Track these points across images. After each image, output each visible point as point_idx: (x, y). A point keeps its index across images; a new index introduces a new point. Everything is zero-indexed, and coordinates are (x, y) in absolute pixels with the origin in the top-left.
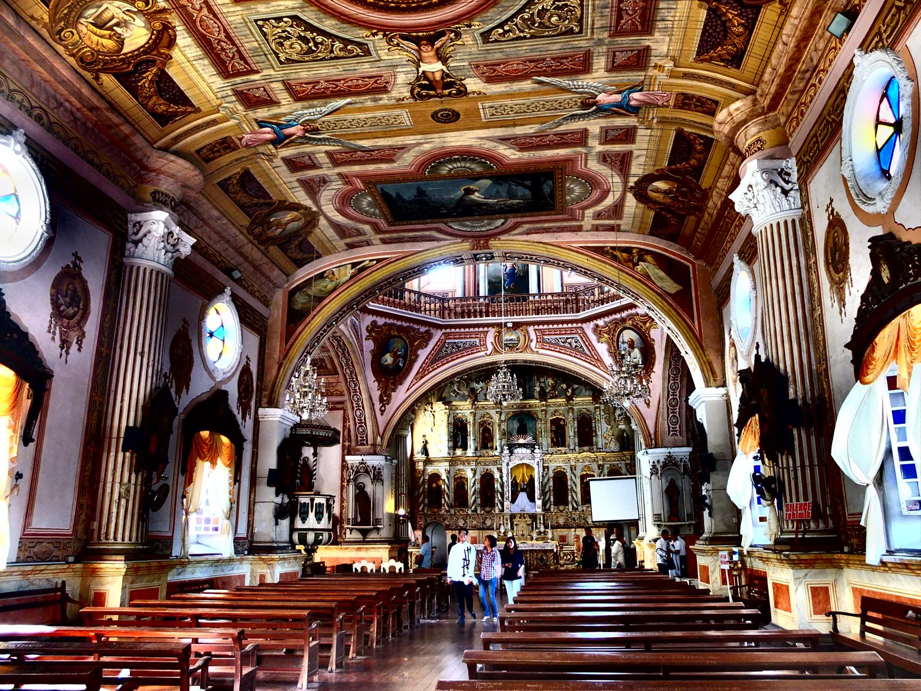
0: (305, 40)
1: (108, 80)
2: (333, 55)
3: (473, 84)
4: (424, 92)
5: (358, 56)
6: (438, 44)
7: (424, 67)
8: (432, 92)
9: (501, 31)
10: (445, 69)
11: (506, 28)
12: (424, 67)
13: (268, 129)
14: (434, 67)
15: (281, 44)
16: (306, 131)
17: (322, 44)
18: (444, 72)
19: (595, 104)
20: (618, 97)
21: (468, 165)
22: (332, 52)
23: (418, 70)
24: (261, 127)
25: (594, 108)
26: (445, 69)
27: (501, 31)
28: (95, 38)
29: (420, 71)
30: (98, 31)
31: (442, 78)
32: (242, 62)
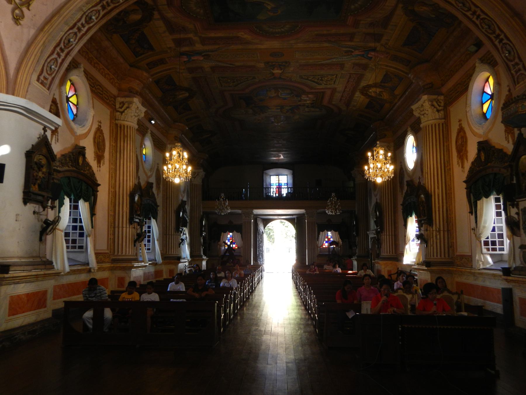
0: (322, 80)
1: (397, 92)
2: (314, 76)
3: (262, 65)
4: (284, 64)
5: (305, 76)
6: (272, 77)
7: (280, 72)
8: (280, 64)
9: (248, 79)
10: (272, 71)
11: (246, 80)
12: (280, 72)
13: (369, 56)
14: (277, 71)
15: (331, 79)
16: (352, 52)
17: (316, 79)
18: (273, 70)
19: (203, 56)
20: (193, 58)
21: (271, 30)
22: (314, 77)
23: (284, 70)
24: (372, 58)
25: (203, 54)
26: (272, 71)
27: (248, 79)
28: (385, 96)
29: (282, 71)
30: (383, 96)
31: (274, 68)
32: (352, 76)
